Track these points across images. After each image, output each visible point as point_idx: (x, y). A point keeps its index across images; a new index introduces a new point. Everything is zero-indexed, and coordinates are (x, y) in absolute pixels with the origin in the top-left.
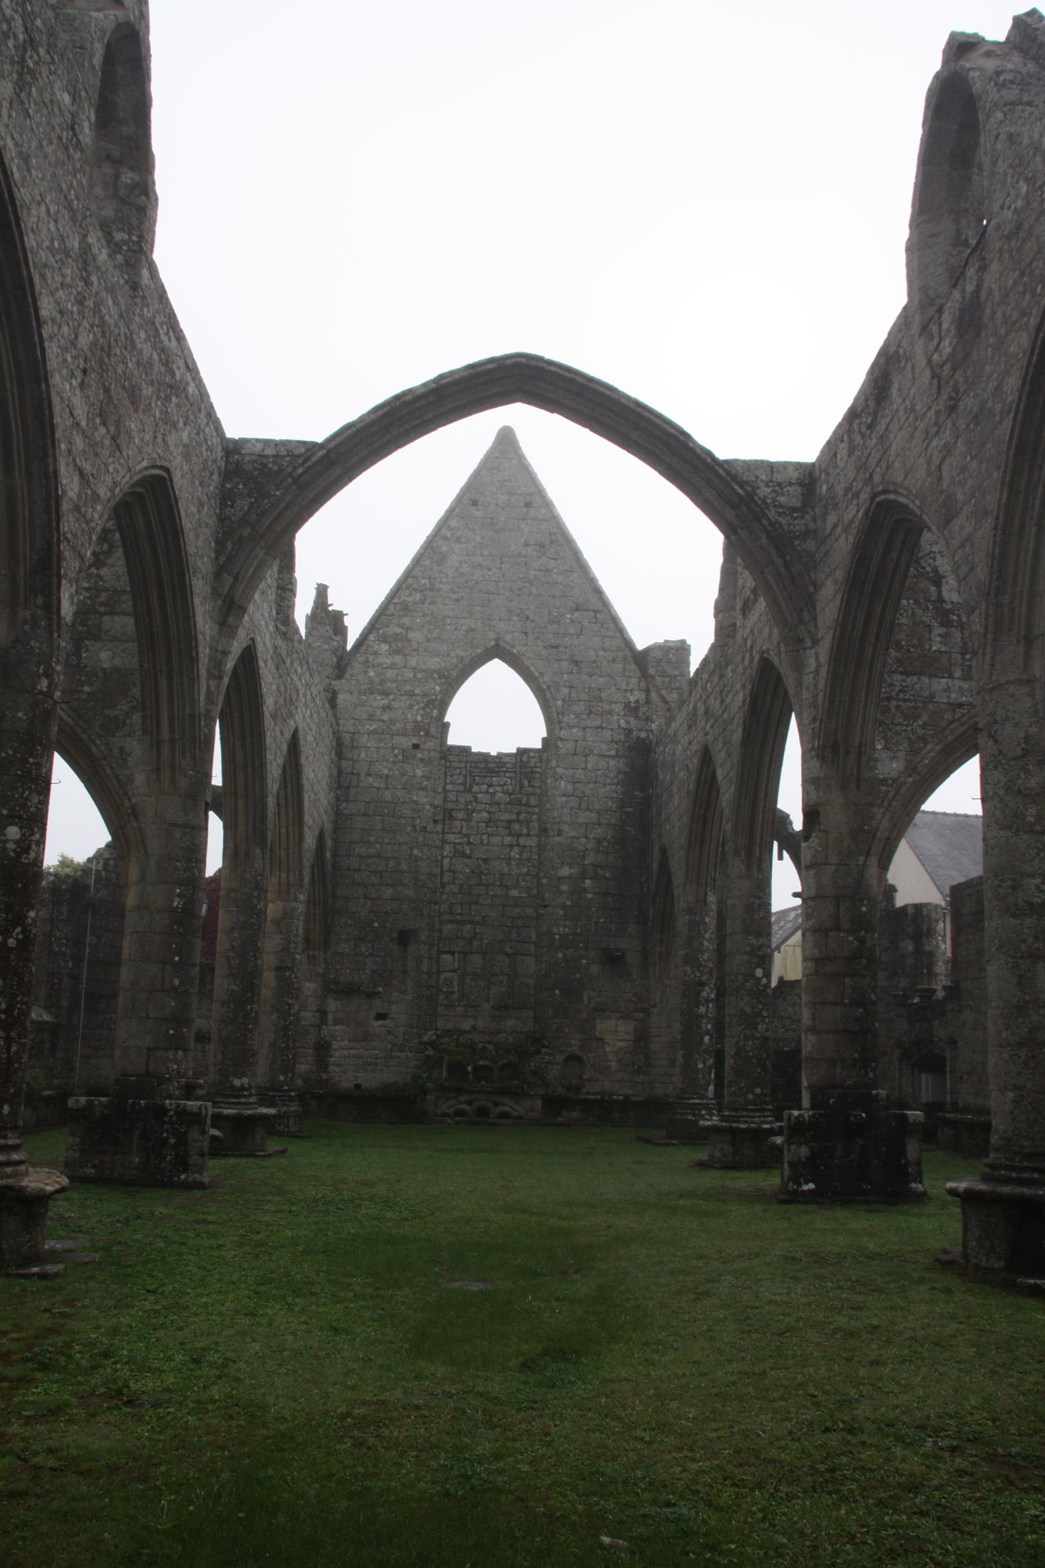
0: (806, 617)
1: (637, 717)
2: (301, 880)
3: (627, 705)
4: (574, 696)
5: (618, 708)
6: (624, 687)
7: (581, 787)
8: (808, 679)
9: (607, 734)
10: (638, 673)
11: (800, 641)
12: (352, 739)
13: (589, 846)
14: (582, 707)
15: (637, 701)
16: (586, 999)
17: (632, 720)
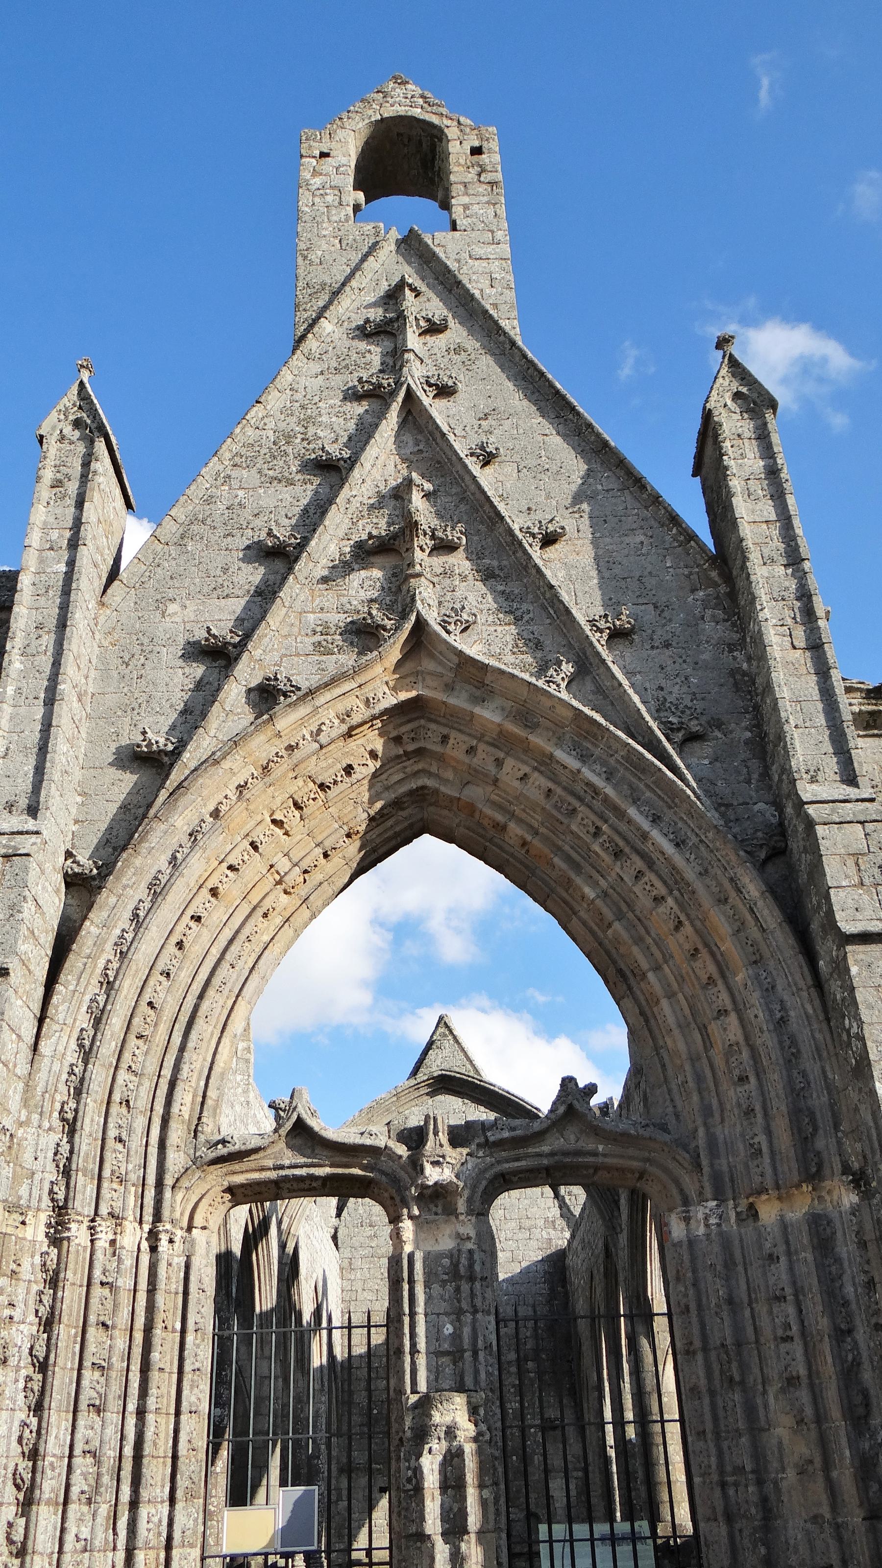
0: (616, 1214)
1: (554, 1228)
2: (323, 1386)
3: (546, 1220)
4: (508, 1216)
5: (540, 1223)
6: (543, 1205)
7: (518, 1286)
8: (621, 1253)
9: (534, 1244)
10: (552, 1194)
11: (614, 1228)
12: (350, 1264)
13: (528, 1334)
14: (513, 1224)
15: (554, 1216)
16: (536, 1462)
17: (550, 1230)
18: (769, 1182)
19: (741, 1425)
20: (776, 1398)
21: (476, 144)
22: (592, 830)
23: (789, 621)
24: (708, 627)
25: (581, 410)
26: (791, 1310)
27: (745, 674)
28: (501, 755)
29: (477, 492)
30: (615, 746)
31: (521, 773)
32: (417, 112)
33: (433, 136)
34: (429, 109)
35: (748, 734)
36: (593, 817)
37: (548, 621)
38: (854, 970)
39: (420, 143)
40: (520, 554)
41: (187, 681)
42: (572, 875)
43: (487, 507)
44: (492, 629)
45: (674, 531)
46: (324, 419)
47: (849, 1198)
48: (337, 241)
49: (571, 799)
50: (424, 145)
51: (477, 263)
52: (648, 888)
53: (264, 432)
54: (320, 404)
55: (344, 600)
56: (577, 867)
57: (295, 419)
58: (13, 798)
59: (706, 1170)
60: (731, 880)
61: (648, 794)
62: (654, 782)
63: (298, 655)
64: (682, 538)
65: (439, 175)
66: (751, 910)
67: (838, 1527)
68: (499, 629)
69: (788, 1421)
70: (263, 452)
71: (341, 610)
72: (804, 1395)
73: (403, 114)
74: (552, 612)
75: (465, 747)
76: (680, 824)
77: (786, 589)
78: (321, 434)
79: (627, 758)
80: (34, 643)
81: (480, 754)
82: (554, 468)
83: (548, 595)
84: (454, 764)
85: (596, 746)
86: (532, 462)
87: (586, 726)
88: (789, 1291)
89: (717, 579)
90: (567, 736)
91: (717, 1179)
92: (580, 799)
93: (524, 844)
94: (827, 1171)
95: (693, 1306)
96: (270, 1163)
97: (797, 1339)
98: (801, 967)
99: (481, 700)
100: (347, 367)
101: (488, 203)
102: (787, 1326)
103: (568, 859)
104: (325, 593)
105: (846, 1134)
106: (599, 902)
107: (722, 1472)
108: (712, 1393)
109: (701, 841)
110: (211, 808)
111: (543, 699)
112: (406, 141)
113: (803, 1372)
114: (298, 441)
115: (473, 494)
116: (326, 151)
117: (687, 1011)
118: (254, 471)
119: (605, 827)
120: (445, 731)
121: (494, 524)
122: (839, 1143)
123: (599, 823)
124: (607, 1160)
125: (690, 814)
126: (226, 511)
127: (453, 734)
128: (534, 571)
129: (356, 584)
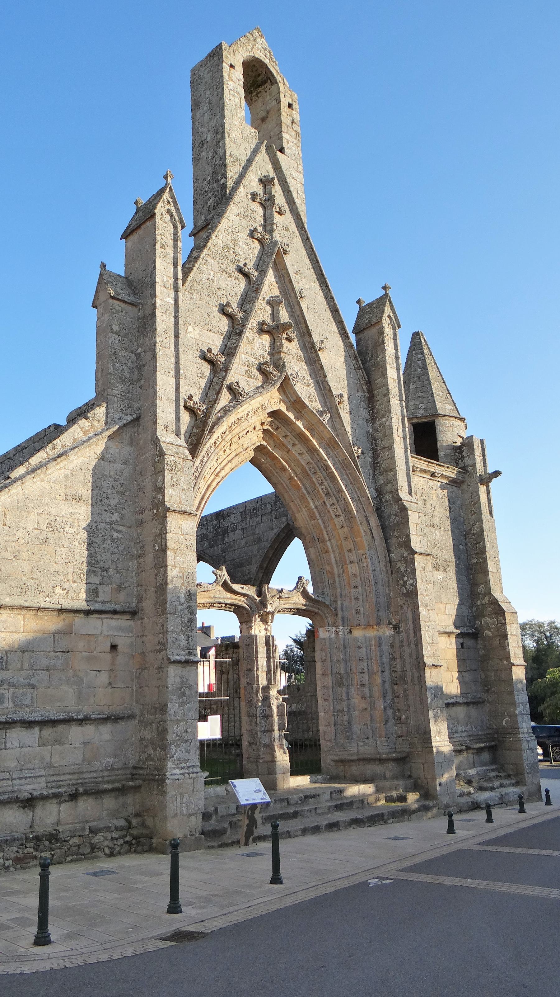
18: (362, 623)
19: (344, 697)
20: (355, 690)
21: (291, 102)
22: (320, 482)
23: (398, 425)
24: (362, 409)
25: (331, 289)
26: (365, 664)
27: (371, 434)
28: (297, 442)
29: (300, 316)
30: (341, 454)
31: (301, 452)
32: (267, 61)
33: (268, 78)
34: (272, 63)
35: (370, 460)
36: (323, 479)
37: (319, 389)
38: (416, 564)
39: (259, 75)
40: (314, 355)
41: (199, 372)
42: (307, 496)
43: (303, 326)
44: (302, 386)
45: (354, 361)
46: (240, 243)
47: (389, 632)
48: (240, 132)
49: (317, 468)
50: (261, 77)
51: (293, 180)
52: (335, 510)
53: (218, 240)
54: (239, 234)
55: (254, 352)
56: (309, 493)
57: (229, 239)
58: (166, 424)
59: (340, 615)
60: (366, 516)
61: (345, 476)
62: (350, 473)
63: (240, 374)
64: (356, 366)
65: (257, 94)
66: (370, 529)
67: (372, 727)
68: (305, 387)
69: (359, 697)
70: (219, 252)
71: (253, 356)
72: (366, 690)
73: (263, 60)
74: (322, 387)
75: (284, 434)
76: (353, 491)
77: (397, 410)
78: (240, 253)
79: (343, 460)
80: (165, 341)
81: (288, 438)
82: (319, 313)
83: (321, 379)
84: (276, 439)
85: (332, 451)
86: (312, 307)
87: (333, 442)
88: (365, 658)
89: (365, 389)
90: (323, 444)
91: (343, 618)
92: (319, 468)
93: (291, 478)
94: (382, 623)
95: (328, 660)
96: (212, 596)
97: (366, 673)
98: (385, 554)
99: (297, 418)
100: (247, 216)
101: (296, 144)
102: (363, 669)
103: (306, 489)
104: (248, 345)
105: (391, 612)
106: (315, 510)
107: (334, 712)
108: (333, 688)
109: (359, 500)
110: (213, 442)
111: (321, 427)
112: (254, 70)
113: (367, 683)
114: (232, 252)
115: (298, 316)
116: (233, 64)
117: (338, 559)
118: (216, 263)
119: (326, 483)
120: (279, 425)
121: (305, 335)
122: (388, 615)
123: (324, 481)
124: (310, 608)
125: (358, 488)
126: (207, 281)
127: (282, 427)
128: (318, 366)
129: (257, 344)
